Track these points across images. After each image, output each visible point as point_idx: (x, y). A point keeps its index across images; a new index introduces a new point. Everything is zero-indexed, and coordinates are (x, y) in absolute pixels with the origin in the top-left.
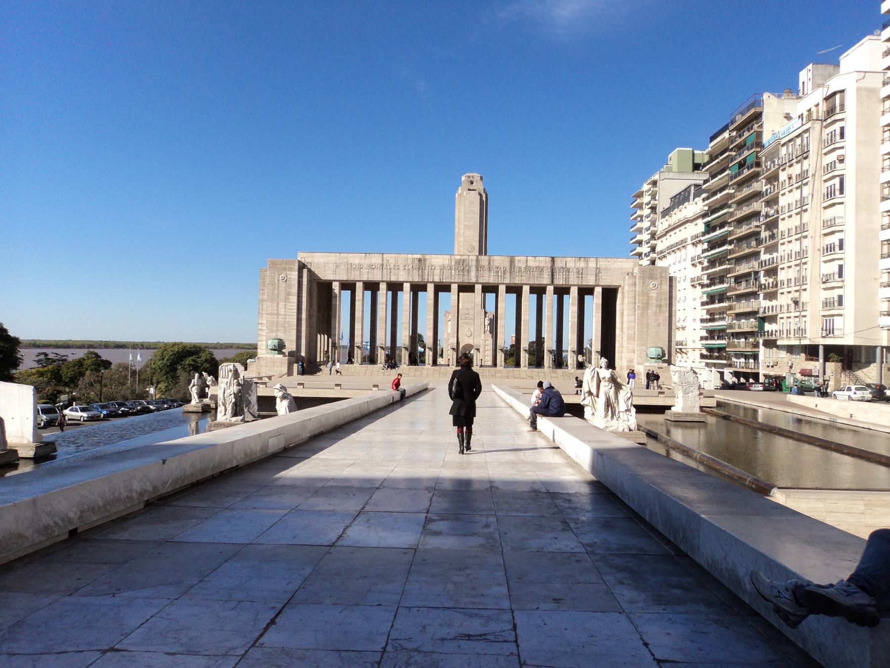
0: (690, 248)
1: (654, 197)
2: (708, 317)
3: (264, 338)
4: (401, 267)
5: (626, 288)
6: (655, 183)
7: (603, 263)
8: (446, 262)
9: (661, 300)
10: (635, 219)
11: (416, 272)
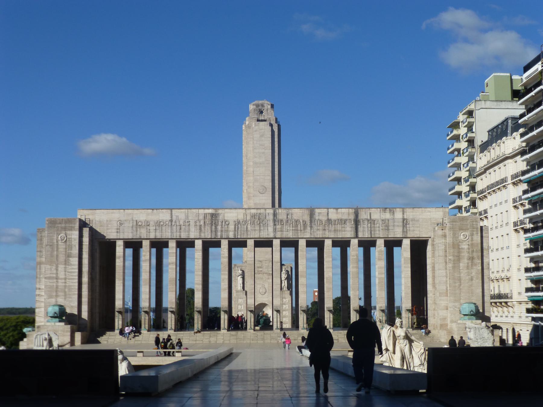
0: (511, 187)
1: (470, 127)
2: (533, 265)
3: (43, 304)
4: (192, 223)
5: (437, 241)
6: (470, 114)
7: (410, 214)
8: (241, 217)
9: (473, 251)
10: (452, 152)
11: (208, 228)
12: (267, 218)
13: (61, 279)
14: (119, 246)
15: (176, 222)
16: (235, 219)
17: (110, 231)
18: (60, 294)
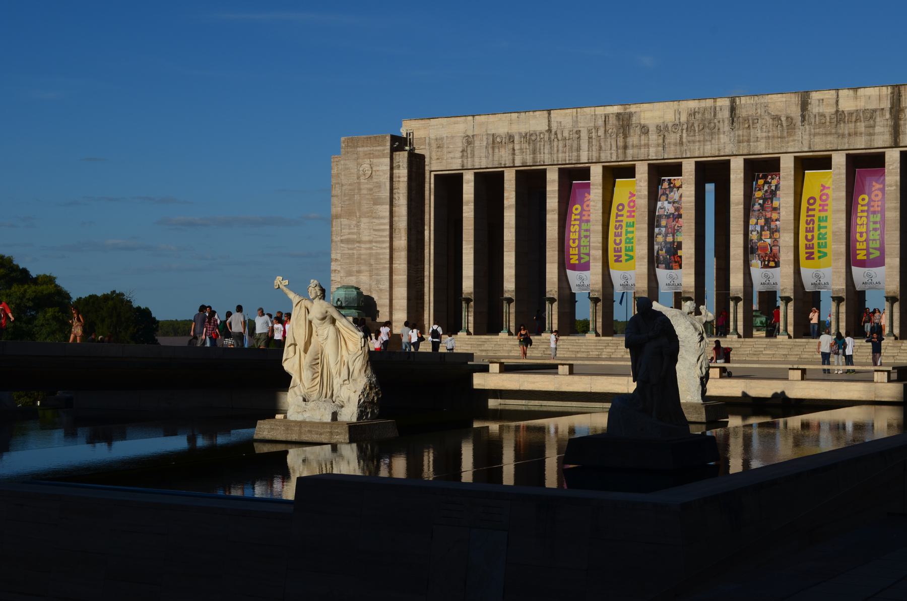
4: (584, 135)
12: (720, 115)
13: (365, 242)
14: (468, 183)
15: (556, 134)
16: (659, 121)
17: (451, 155)
18: (363, 268)
